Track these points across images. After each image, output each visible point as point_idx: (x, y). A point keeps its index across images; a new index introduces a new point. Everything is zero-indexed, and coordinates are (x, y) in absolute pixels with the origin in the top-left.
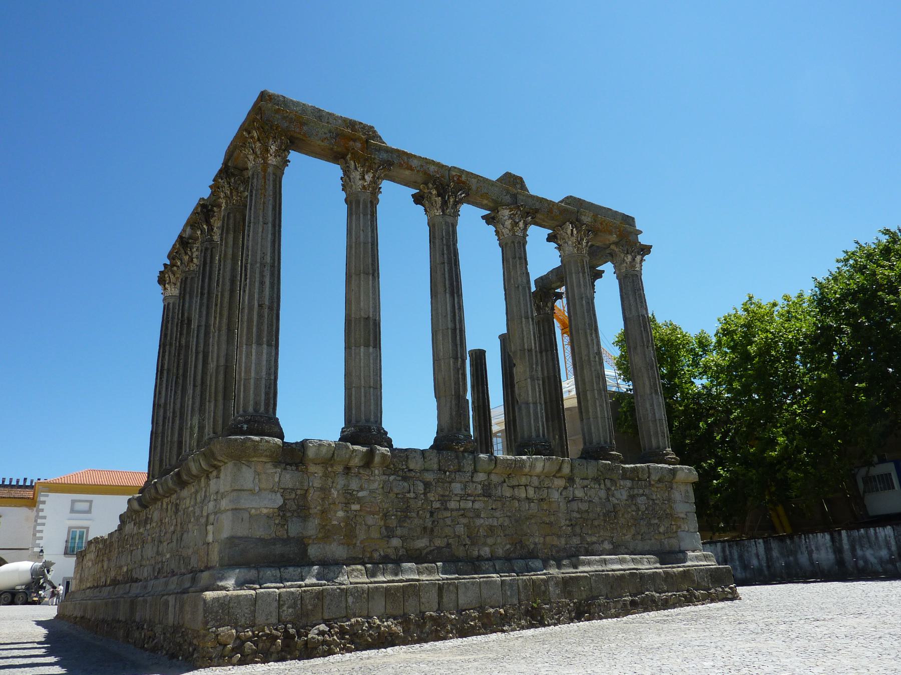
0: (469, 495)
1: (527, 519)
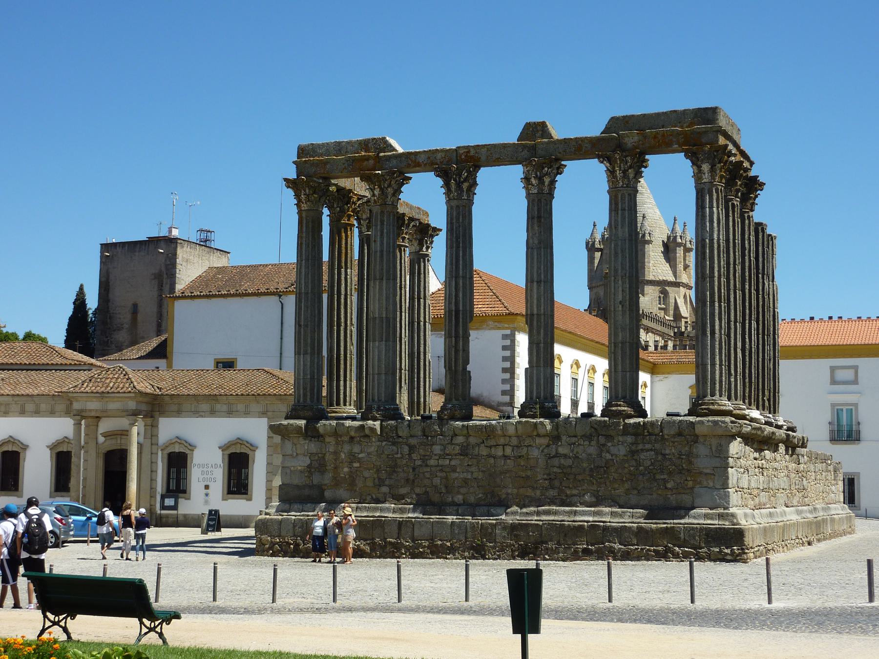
0: (448, 455)
1: (501, 473)
